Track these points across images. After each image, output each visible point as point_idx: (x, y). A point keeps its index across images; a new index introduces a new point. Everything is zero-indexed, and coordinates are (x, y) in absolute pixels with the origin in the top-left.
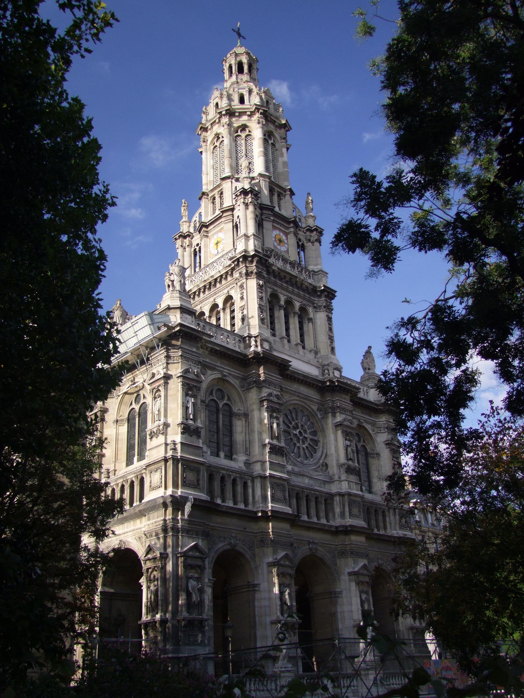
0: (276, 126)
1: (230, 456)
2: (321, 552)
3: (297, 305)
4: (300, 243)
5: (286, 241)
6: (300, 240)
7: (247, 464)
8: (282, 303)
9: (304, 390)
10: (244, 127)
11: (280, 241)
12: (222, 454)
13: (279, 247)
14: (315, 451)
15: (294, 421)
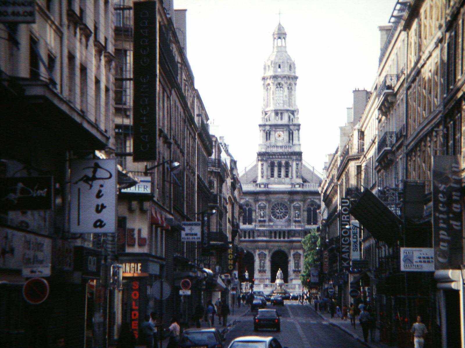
0: (282, 78)
1: (250, 223)
2: (282, 249)
3: (283, 162)
4: (291, 132)
5: (283, 135)
6: (291, 130)
7: (255, 226)
8: (276, 164)
9: (281, 196)
10: (269, 84)
11: (280, 136)
12: (247, 224)
13: (279, 139)
14: (286, 215)
15: (276, 207)
